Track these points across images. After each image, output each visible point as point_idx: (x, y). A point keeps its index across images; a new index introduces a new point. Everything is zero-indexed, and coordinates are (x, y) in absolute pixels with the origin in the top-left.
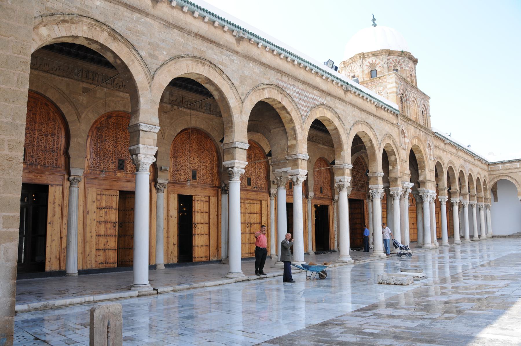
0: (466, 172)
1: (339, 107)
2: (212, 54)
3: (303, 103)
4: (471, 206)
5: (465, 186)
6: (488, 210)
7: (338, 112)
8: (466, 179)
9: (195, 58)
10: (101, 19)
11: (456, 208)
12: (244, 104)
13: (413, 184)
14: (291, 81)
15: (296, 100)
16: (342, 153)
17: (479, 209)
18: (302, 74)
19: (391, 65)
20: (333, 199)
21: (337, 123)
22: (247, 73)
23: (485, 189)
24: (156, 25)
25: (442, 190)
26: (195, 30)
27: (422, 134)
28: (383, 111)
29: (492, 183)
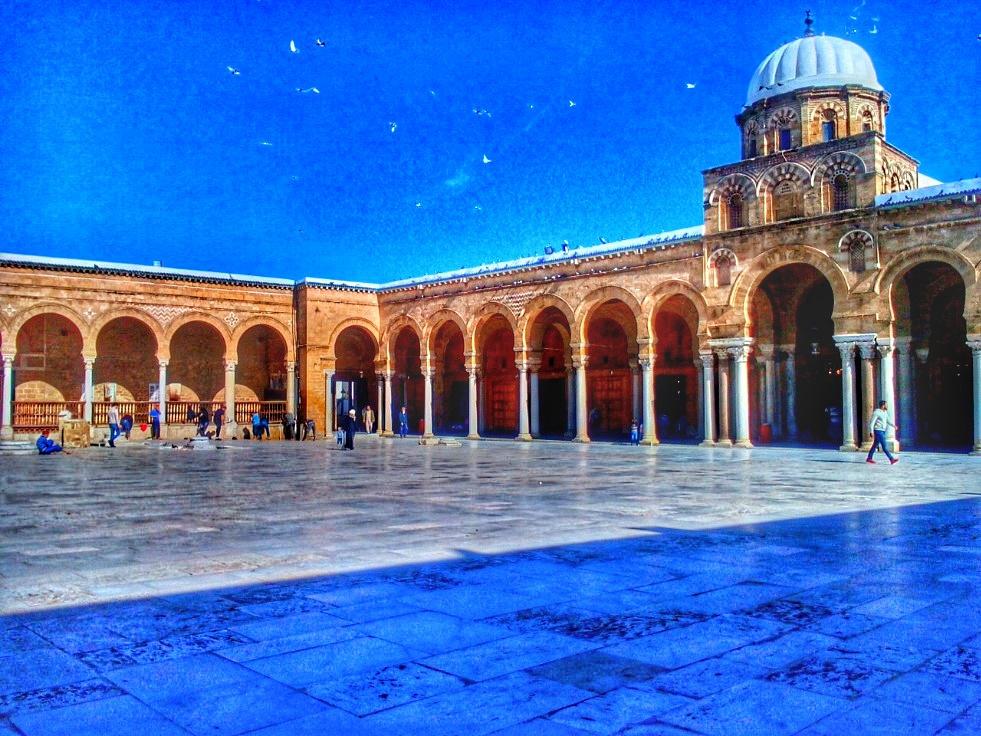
27: (813, 232)
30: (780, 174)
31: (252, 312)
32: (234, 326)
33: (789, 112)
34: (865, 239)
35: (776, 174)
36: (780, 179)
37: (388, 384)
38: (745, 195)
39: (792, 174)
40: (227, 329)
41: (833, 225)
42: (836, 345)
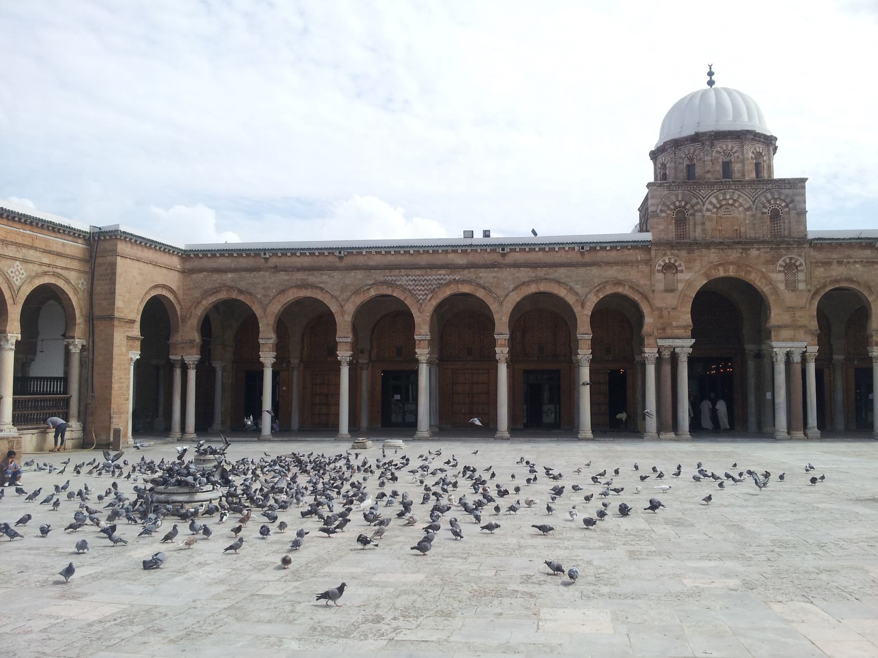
1: (486, 276)
2: (312, 279)
3: (421, 287)
7: (482, 282)
9: (299, 287)
10: (232, 284)
12: (345, 308)
14: (403, 272)
15: (411, 288)
18: (424, 260)
19: (681, 161)
21: (480, 294)
22: (347, 282)
24: (267, 274)
26: (299, 265)
27: (754, 252)
28: (602, 254)
30: (725, 199)
31: (41, 264)
32: (18, 283)
33: (733, 147)
34: (798, 264)
35: (721, 198)
36: (724, 203)
37: (192, 374)
38: (691, 212)
39: (735, 201)
40: (10, 287)
41: (771, 249)
42: (775, 350)
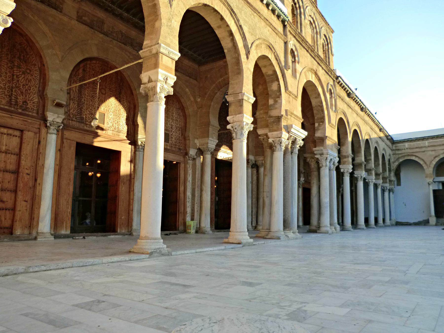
0: (372, 143)
4: (376, 186)
5: (371, 160)
6: (391, 193)
8: (372, 151)
11: (361, 185)
13: (306, 133)
16: (157, 24)
17: (383, 191)
20: (187, 154)
23: (390, 171)
25: (345, 157)
29: (397, 163)
